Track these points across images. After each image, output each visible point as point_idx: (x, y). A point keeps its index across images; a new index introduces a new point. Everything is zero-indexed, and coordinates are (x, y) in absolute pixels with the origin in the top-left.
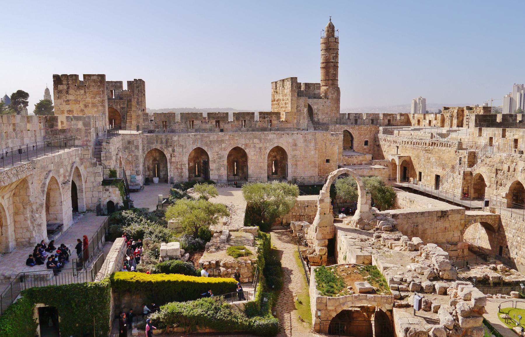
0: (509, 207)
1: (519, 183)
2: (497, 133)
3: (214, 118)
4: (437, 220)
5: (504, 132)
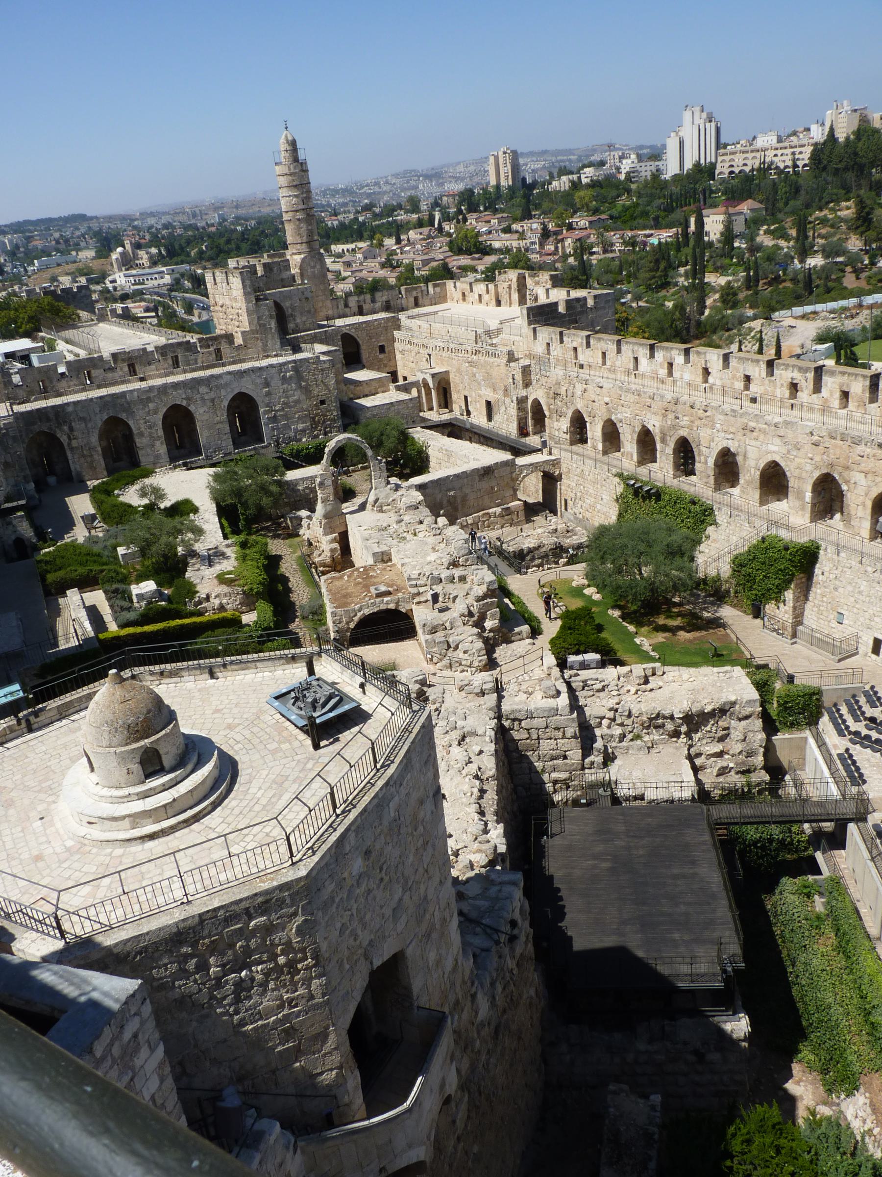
0: (572, 443)
1: (579, 412)
2: (554, 337)
3: (123, 360)
4: (480, 480)
5: (561, 333)
